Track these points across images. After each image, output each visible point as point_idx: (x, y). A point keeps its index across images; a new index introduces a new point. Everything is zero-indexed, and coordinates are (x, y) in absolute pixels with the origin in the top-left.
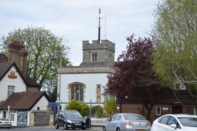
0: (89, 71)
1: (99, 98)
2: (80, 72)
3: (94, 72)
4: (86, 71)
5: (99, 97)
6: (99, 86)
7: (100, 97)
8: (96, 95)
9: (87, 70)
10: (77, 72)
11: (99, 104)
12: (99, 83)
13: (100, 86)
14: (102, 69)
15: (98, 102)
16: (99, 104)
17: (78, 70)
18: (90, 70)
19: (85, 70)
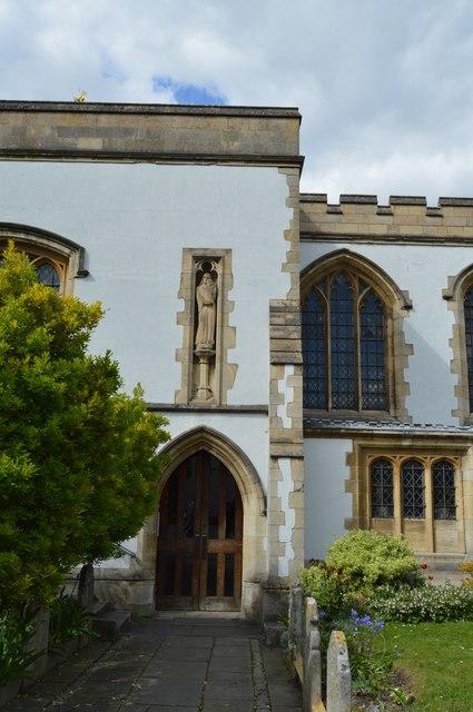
0: (119, 144)
1: (203, 368)
2: (39, 145)
3: (169, 147)
4: (96, 144)
5: (204, 357)
6: (206, 266)
7: (211, 361)
8: (178, 336)
9: (99, 132)
10: (13, 146)
11: (215, 423)
12: (208, 243)
13: (218, 268)
14: (234, 136)
15: (201, 398)
16: (215, 423)
17: (21, 132)
18: (127, 132)
19: (84, 132)
